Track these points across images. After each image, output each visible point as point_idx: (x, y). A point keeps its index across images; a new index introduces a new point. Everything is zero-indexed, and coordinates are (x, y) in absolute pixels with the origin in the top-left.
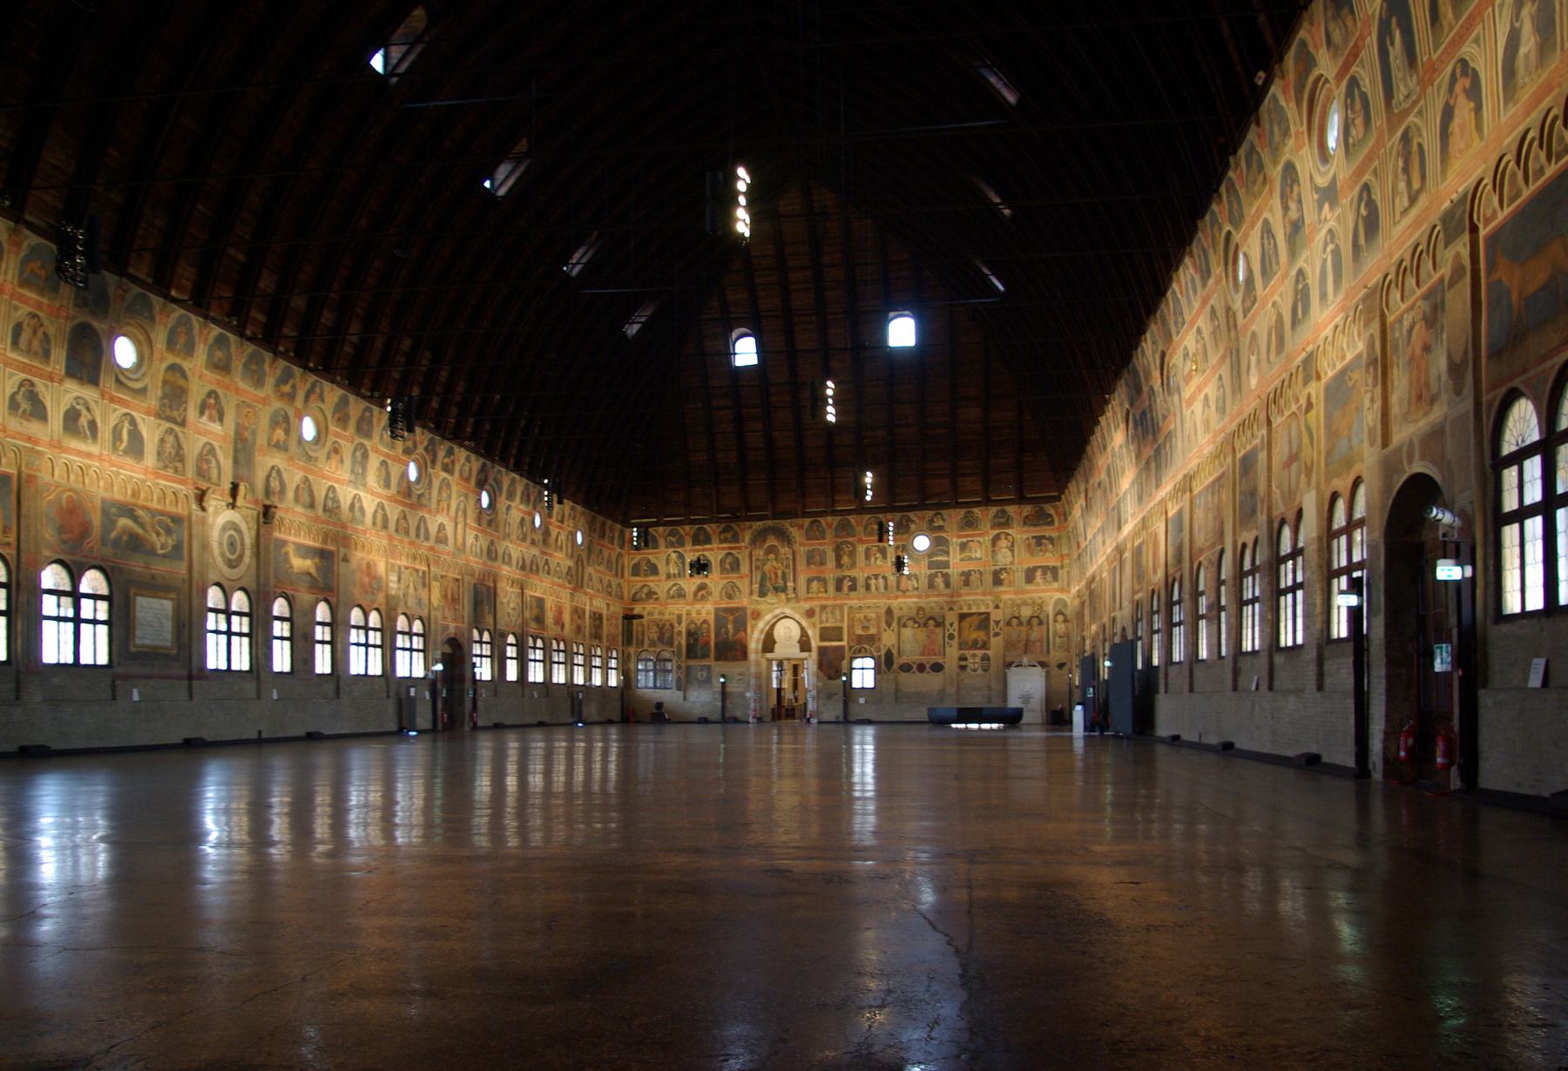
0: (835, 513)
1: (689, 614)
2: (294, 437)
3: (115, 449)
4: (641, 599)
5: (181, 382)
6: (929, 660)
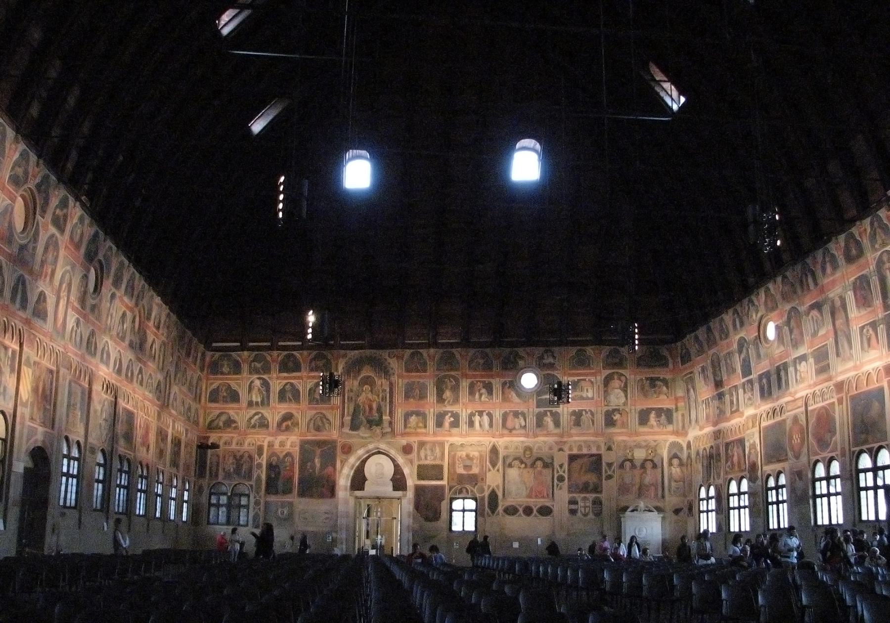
0: (435, 345)
1: (271, 445)
4: (218, 428)
6: (536, 503)
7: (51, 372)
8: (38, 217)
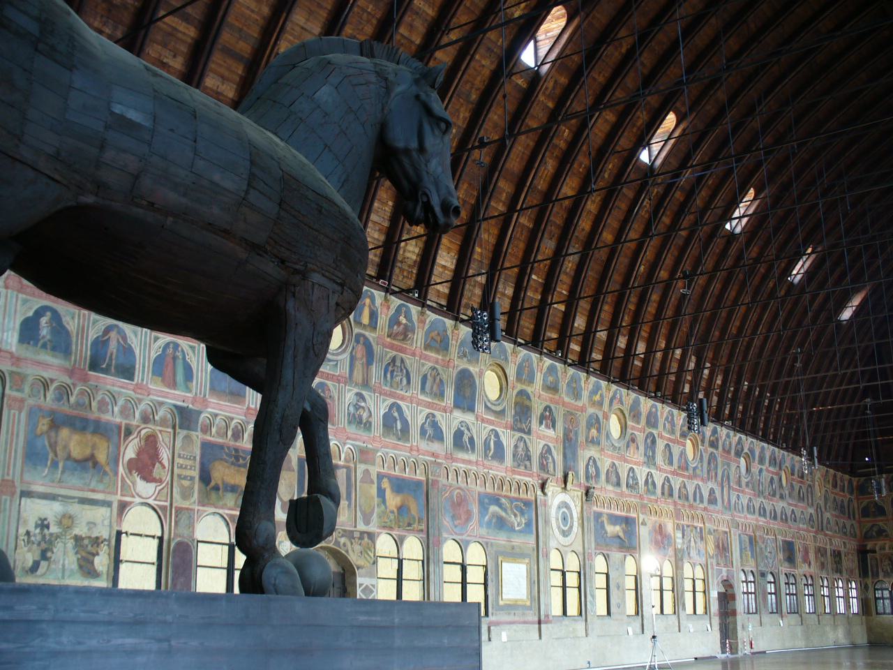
2: (604, 433)
3: (486, 456)
5: (527, 403)
7: (726, 533)
8: (700, 447)
